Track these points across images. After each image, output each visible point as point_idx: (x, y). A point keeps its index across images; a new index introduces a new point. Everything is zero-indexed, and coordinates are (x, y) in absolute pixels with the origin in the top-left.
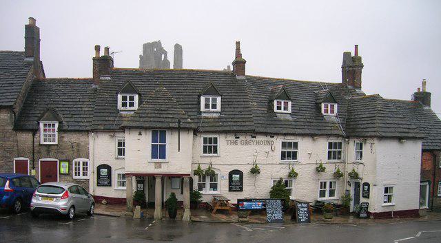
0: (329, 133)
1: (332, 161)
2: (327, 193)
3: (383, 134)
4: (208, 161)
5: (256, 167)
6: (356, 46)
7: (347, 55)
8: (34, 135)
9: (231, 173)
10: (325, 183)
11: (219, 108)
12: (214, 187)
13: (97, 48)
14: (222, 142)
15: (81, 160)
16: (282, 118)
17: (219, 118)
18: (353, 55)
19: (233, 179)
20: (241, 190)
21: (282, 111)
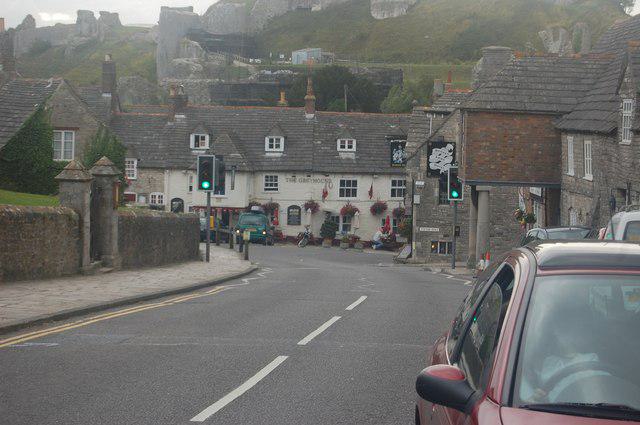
1: (397, 198)
9: (290, 208)
11: (282, 149)
14: (282, 179)
15: (157, 194)
17: (282, 157)
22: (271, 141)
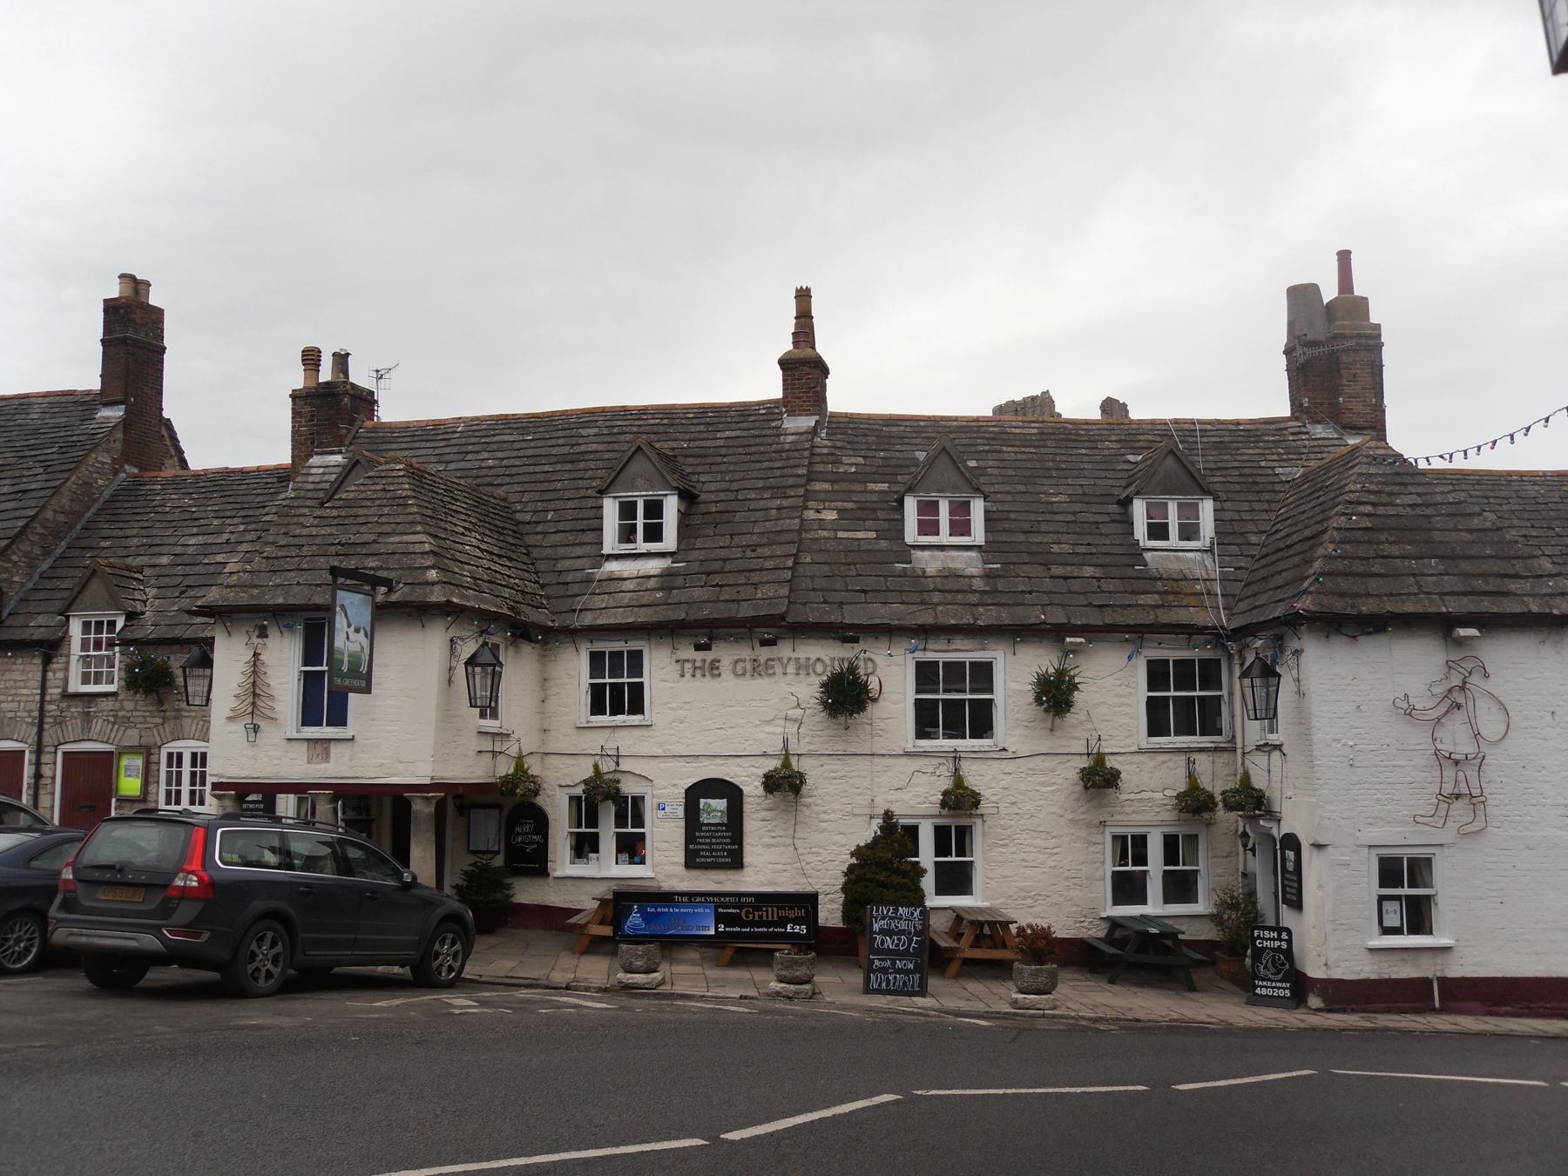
0: (1148, 618)
2: (1155, 888)
3: (1338, 606)
4: (593, 742)
5: (786, 764)
6: (1344, 258)
7: (1302, 297)
8: (47, 661)
9: (698, 792)
10: (1140, 841)
11: (670, 540)
12: (631, 848)
13: (311, 358)
15: (187, 747)
16: (931, 569)
17: (667, 574)
18: (1329, 292)
19: (704, 819)
20: (736, 861)
21: (944, 537)
22: (627, 510)
